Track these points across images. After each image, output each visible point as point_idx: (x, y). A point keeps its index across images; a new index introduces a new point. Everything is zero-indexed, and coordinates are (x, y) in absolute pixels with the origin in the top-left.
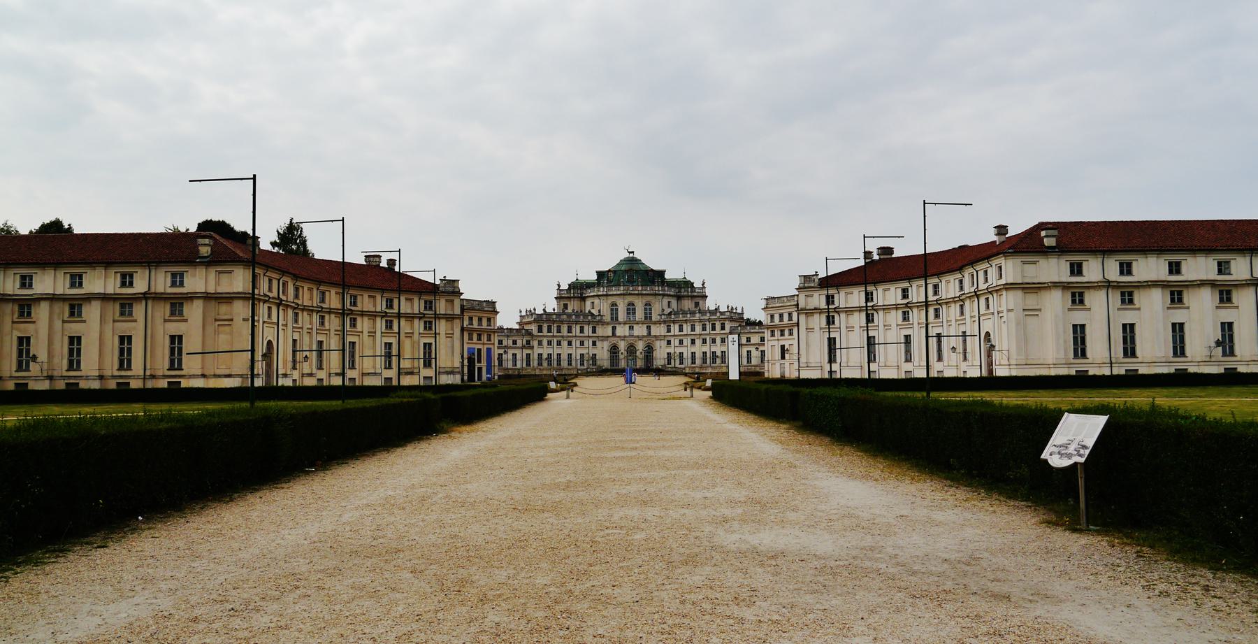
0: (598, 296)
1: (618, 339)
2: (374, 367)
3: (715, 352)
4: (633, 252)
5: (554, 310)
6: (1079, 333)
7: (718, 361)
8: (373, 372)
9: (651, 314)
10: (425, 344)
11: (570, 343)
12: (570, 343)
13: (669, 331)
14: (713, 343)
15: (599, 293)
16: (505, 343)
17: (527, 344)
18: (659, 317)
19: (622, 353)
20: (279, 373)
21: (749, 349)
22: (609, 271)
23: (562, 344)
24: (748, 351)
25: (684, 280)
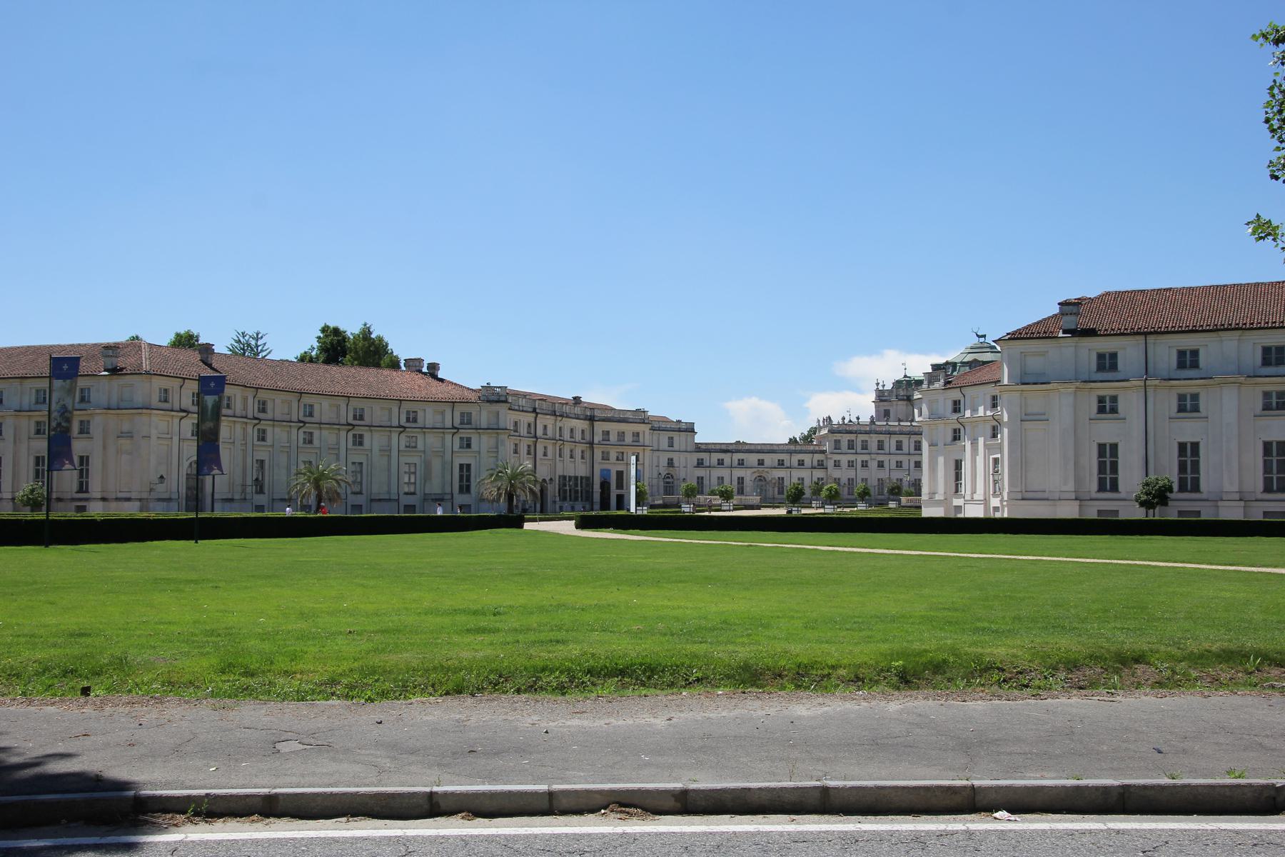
2: (389, 493)
4: (984, 336)
5: (858, 418)
6: (1108, 456)
8: (388, 498)
10: (461, 466)
11: (881, 465)
12: (881, 465)
16: (787, 463)
17: (819, 465)
20: (216, 496)
23: (869, 464)
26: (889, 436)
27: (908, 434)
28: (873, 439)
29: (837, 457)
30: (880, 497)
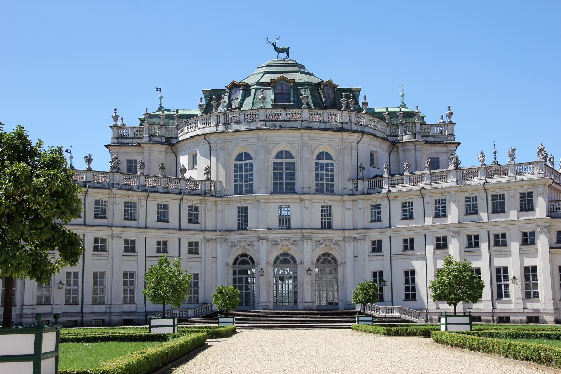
3: (506, 270)
4: (286, 50)
5: (89, 160)
9: (331, 178)
13: (376, 217)
14: (497, 244)
15: (207, 130)
18: (350, 186)
19: (262, 273)
22: (233, 87)
23: (109, 246)
25: (403, 110)
26: (145, 194)
27: (180, 193)
28: (118, 200)
30: (127, 308)
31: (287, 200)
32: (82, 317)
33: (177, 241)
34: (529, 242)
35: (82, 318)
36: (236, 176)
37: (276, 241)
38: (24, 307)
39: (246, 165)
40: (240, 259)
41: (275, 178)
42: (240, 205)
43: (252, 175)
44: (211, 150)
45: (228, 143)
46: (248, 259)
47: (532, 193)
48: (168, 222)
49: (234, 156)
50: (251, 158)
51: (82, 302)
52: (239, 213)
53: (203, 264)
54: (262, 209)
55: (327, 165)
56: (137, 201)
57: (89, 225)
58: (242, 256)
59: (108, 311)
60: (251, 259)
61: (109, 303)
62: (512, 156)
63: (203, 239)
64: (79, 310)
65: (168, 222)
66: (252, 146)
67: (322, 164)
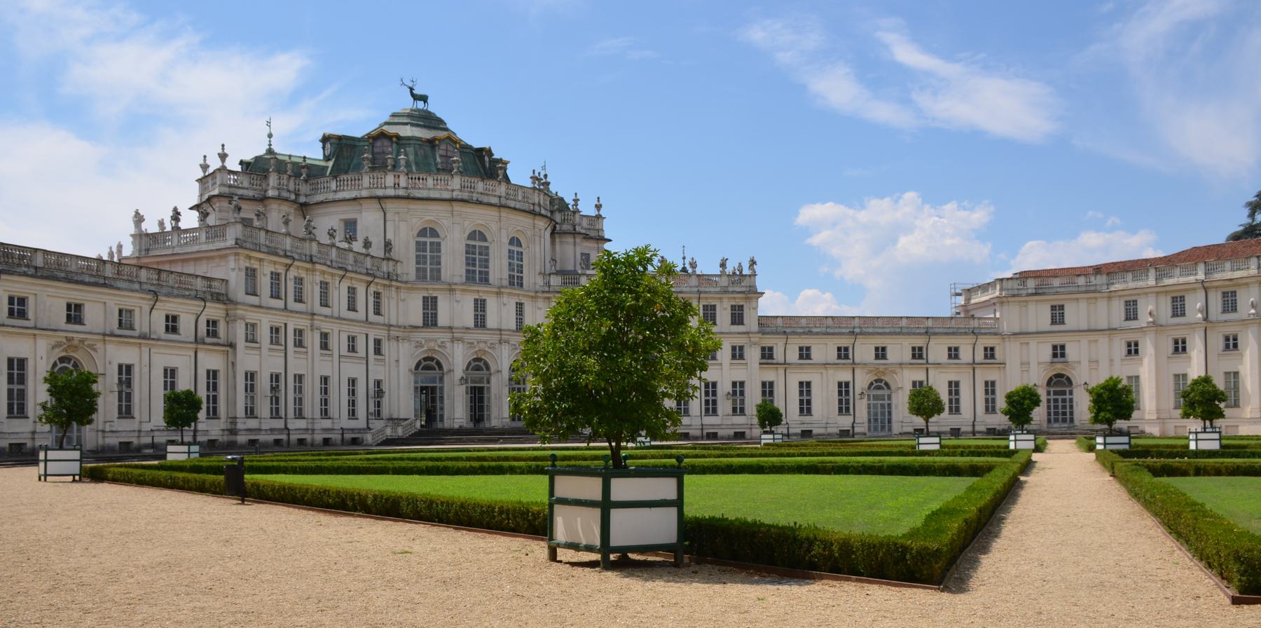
0: (379, 198)
1: (444, 337)
4: (424, 99)
7: (724, 406)
15: (380, 193)
18: (540, 281)
21: (805, 378)
24: (801, 384)
26: (341, 273)
29: (252, 316)
31: (484, 292)
32: (289, 435)
33: (365, 336)
34: (738, 357)
35: (289, 437)
36: (417, 256)
37: (473, 343)
38: (238, 420)
39: (432, 243)
40: (424, 363)
41: (468, 264)
42: (426, 295)
43: (439, 257)
44: (387, 219)
45: (410, 213)
46: (433, 363)
47: (742, 306)
48: (357, 311)
49: (416, 232)
50: (437, 236)
51: (286, 415)
52: (424, 305)
53: (387, 368)
54: (457, 301)
55: (518, 252)
56: (330, 281)
57: (291, 312)
58: (425, 359)
59: (310, 427)
60: (439, 364)
61: (310, 417)
62: (723, 265)
63: (386, 335)
64: (283, 427)
65: (357, 311)
66: (443, 221)
67: (513, 251)
